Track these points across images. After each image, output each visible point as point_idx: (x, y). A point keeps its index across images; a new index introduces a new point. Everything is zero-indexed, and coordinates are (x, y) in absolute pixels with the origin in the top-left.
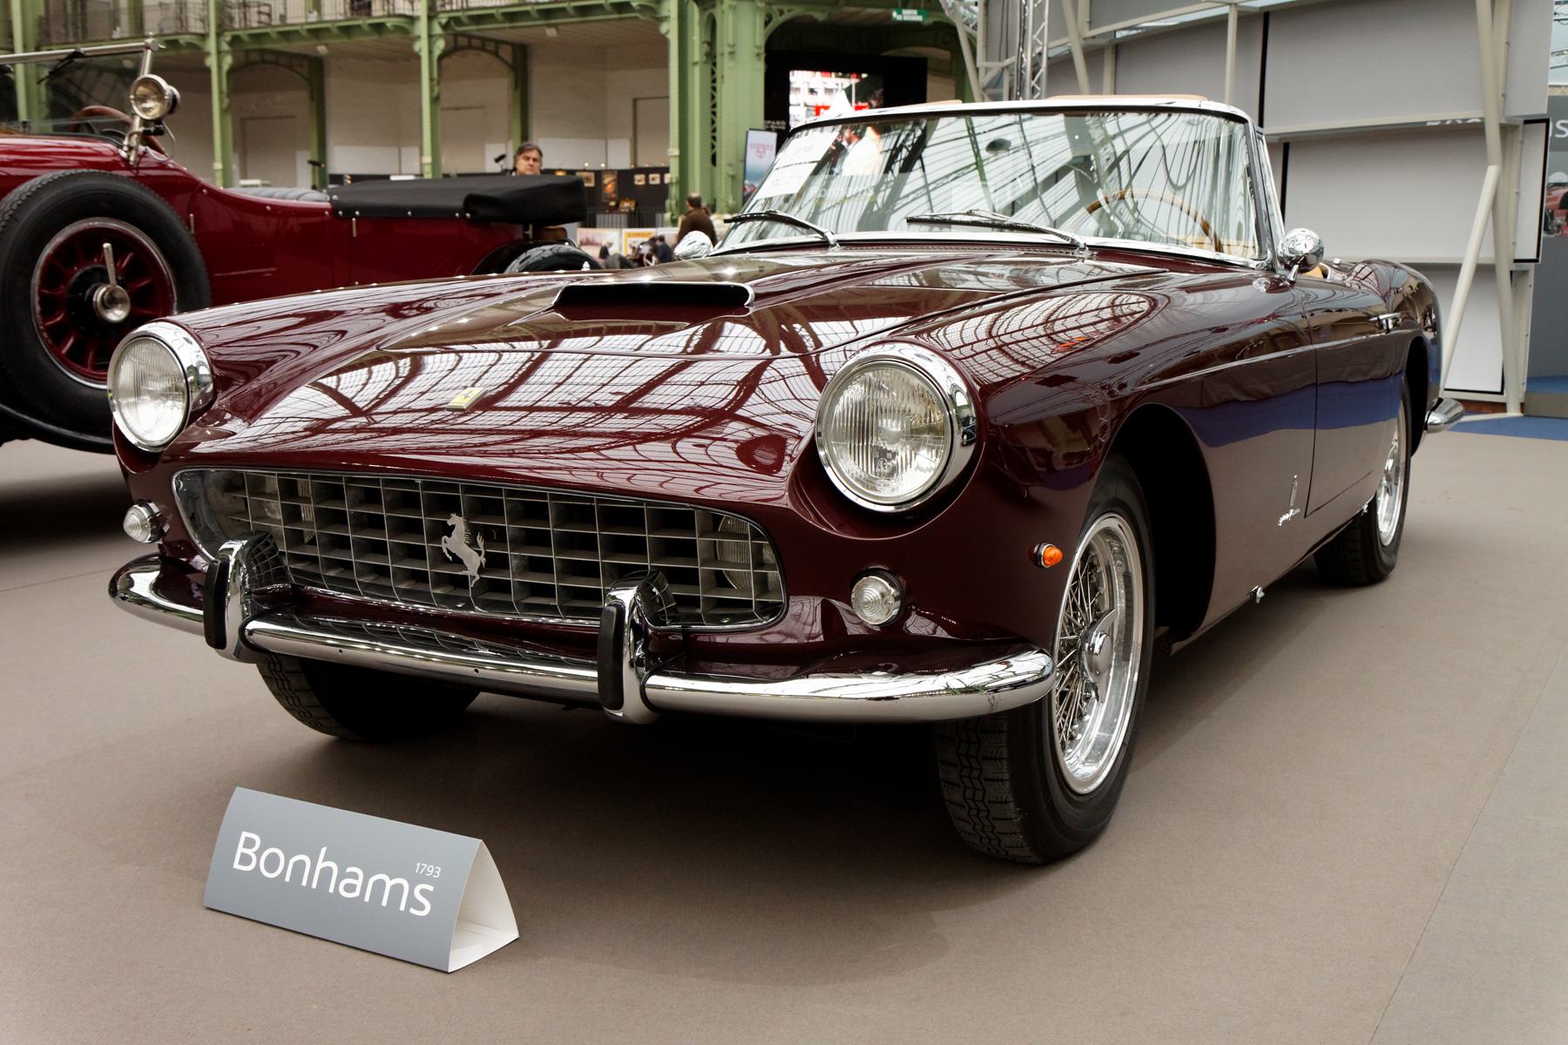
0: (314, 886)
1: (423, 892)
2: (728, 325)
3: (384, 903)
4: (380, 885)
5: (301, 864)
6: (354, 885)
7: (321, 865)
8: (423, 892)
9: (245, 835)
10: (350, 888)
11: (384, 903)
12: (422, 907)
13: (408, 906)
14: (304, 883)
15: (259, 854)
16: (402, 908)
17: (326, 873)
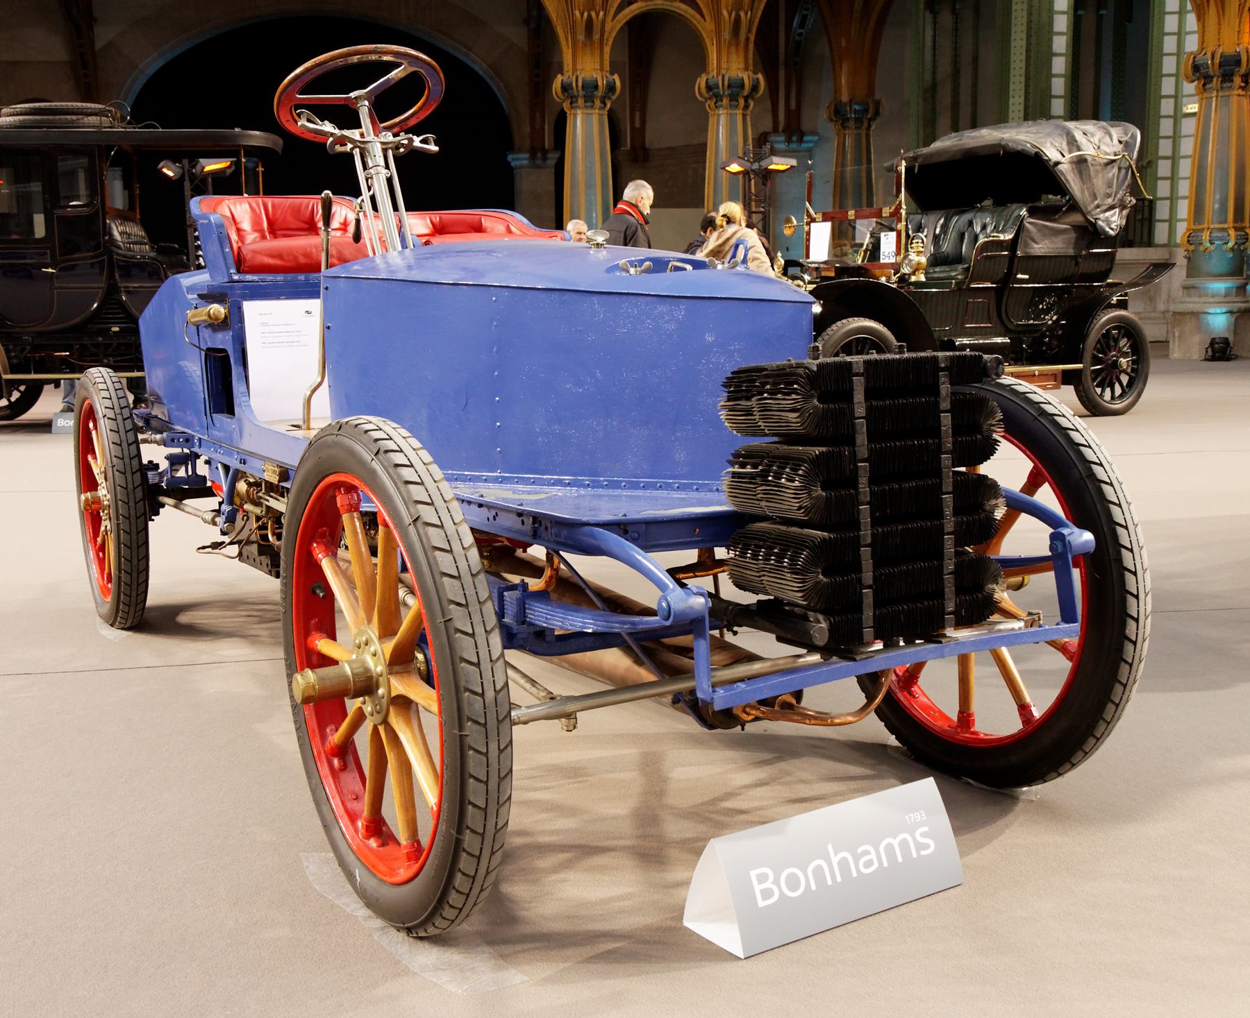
0: (839, 879)
1: (923, 835)
3: (900, 860)
4: (889, 848)
5: (818, 870)
6: (869, 861)
7: (835, 860)
8: (923, 835)
10: (868, 864)
11: (900, 860)
12: (928, 846)
13: (918, 853)
14: (830, 882)
15: (776, 882)
16: (915, 855)
17: (843, 864)
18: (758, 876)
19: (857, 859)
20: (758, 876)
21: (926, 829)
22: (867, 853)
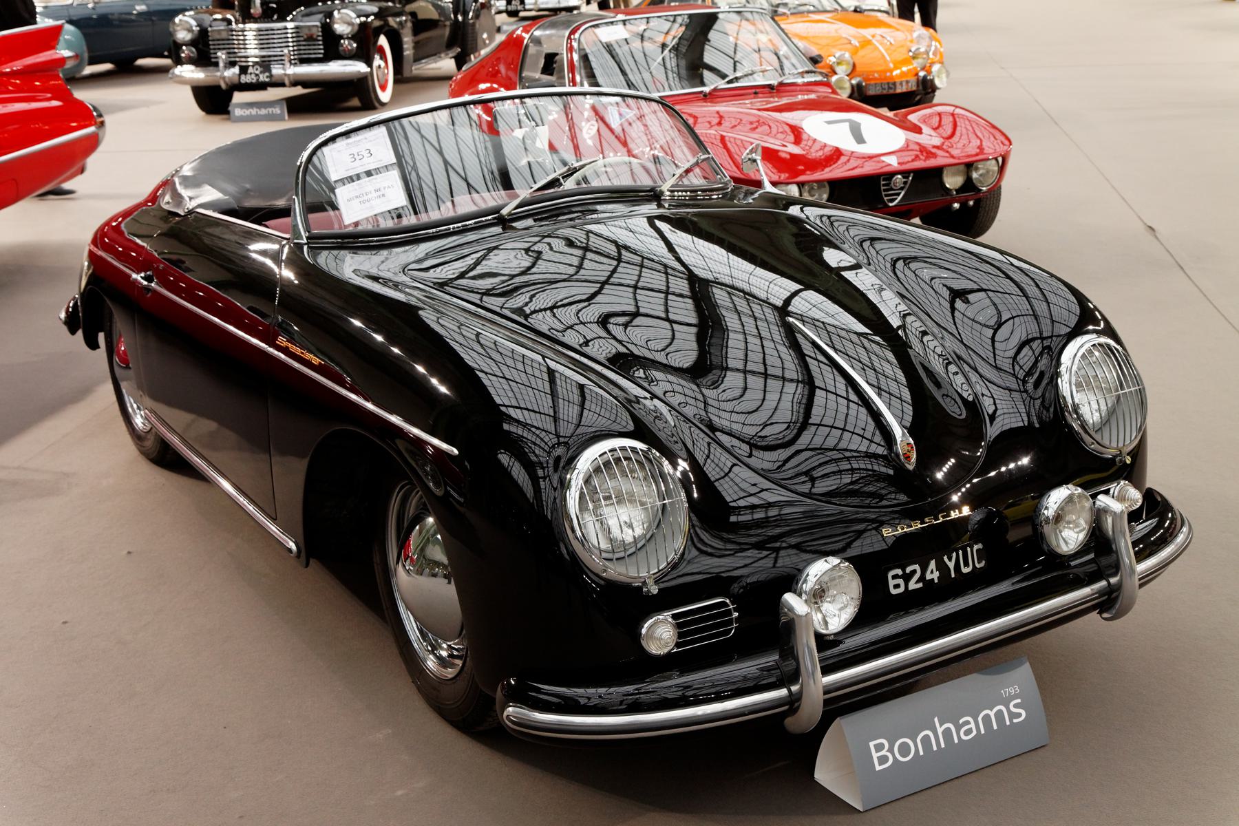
0: (943, 746)
1: (1016, 706)
3: (995, 727)
4: (987, 719)
5: (926, 738)
6: (970, 728)
7: (940, 730)
8: (1016, 706)
10: (968, 732)
11: (995, 727)
17: (947, 733)
18: (875, 746)
20: (875, 746)
22: (968, 723)
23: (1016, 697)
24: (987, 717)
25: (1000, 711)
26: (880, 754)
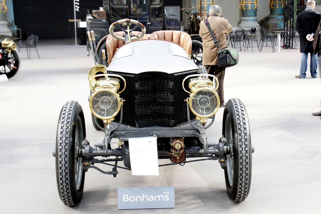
0: (143, 200)
1: (166, 197)
2: (170, 10)
3: (159, 200)
4: (157, 198)
5: (139, 198)
6: (152, 198)
7: (143, 197)
8: (166, 197)
9: (124, 196)
10: (150, 199)
11: (159, 200)
14: (141, 200)
15: (129, 198)
16: (163, 200)
17: (145, 198)
18: (125, 196)
19: (149, 198)
20: (125, 196)
21: (168, 196)
22: (152, 197)
23: (167, 194)
24: (158, 197)
25: (162, 197)
26: (125, 198)
